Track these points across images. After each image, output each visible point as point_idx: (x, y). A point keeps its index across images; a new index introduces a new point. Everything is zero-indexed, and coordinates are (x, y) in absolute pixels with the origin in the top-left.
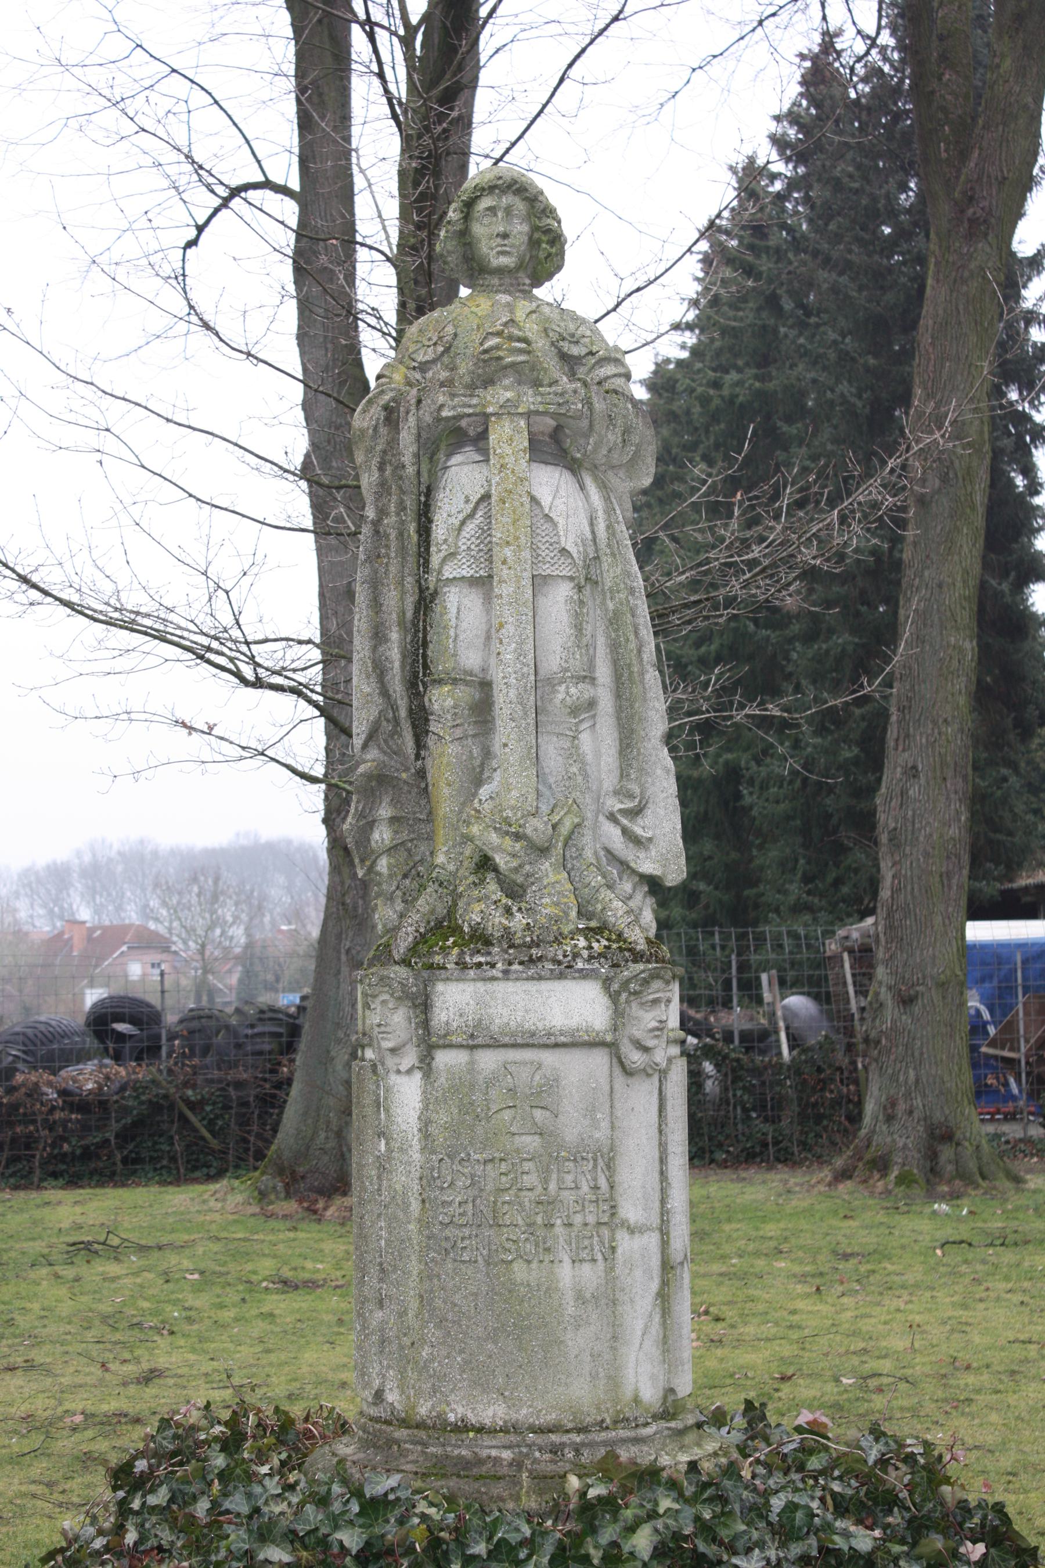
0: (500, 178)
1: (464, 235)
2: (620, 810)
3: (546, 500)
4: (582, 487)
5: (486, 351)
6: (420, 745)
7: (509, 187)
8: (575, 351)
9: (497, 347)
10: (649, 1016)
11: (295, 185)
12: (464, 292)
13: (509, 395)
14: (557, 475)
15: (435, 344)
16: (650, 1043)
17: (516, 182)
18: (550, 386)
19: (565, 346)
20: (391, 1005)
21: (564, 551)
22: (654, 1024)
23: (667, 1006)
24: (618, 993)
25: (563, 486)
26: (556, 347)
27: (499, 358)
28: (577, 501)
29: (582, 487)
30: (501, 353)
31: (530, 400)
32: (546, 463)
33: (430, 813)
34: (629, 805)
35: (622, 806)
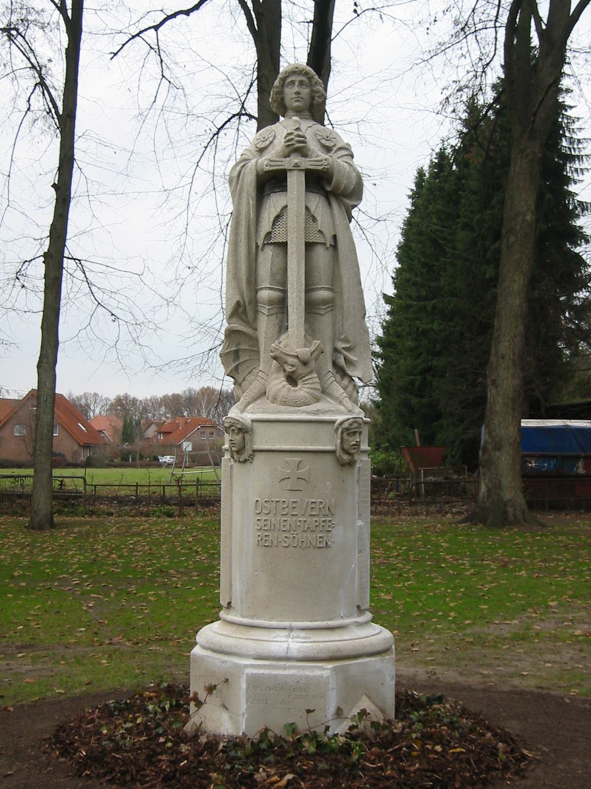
0: (297, 68)
1: (281, 93)
2: (343, 348)
3: (312, 209)
4: (330, 204)
5: (288, 141)
6: (256, 318)
7: (301, 72)
8: (328, 144)
9: (292, 139)
10: (351, 439)
11: (256, 115)
12: (282, 118)
13: (296, 161)
14: (318, 198)
15: (266, 140)
16: (352, 451)
17: (304, 70)
18: (316, 157)
19: (324, 142)
20: (236, 432)
21: (320, 232)
22: (354, 443)
23: (360, 435)
24: (338, 428)
25: (320, 202)
26: (319, 141)
27: (292, 145)
28: (326, 209)
29: (330, 204)
30: (293, 142)
31: (306, 164)
32: (314, 192)
33: (258, 348)
34: (347, 345)
35: (344, 346)
